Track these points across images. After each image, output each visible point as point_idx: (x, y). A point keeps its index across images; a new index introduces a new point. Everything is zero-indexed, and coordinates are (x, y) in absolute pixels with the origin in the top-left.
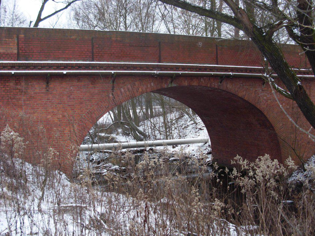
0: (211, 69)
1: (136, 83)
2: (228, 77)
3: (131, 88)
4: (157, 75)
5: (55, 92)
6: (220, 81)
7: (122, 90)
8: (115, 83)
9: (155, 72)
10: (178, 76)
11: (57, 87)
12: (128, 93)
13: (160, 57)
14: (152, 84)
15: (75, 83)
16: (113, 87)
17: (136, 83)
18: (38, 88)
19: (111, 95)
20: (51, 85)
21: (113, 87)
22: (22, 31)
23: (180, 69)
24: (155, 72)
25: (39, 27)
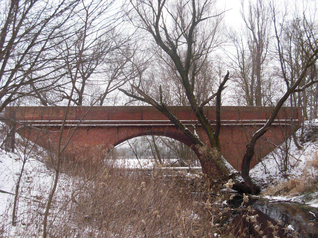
0: (106, 123)
1: (129, 130)
2: (93, 127)
3: (126, 133)
4: (139, 126)
5: (91, 134)
6: (176, 128)
7: (122, 133)
8: (119, 130)
9: (138, 125)
10: (151, 127)
11: (92, 132)
12: (125, 135)
13: (142, 117)
14: (138, 131)
15: (100, 130)
16: (118, 132)
17: (129, 130)
18: (84, 132)
19: (117, 136)
20: (90, 131)
21: (118, 132)
22: (61, 111)
23: (42, 123)
24: (138, 125)
25: (103, 105)
